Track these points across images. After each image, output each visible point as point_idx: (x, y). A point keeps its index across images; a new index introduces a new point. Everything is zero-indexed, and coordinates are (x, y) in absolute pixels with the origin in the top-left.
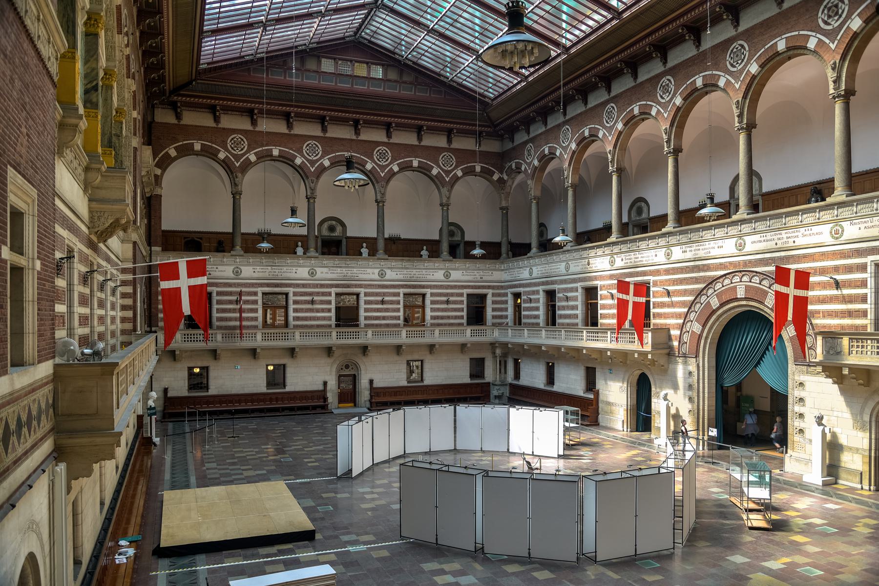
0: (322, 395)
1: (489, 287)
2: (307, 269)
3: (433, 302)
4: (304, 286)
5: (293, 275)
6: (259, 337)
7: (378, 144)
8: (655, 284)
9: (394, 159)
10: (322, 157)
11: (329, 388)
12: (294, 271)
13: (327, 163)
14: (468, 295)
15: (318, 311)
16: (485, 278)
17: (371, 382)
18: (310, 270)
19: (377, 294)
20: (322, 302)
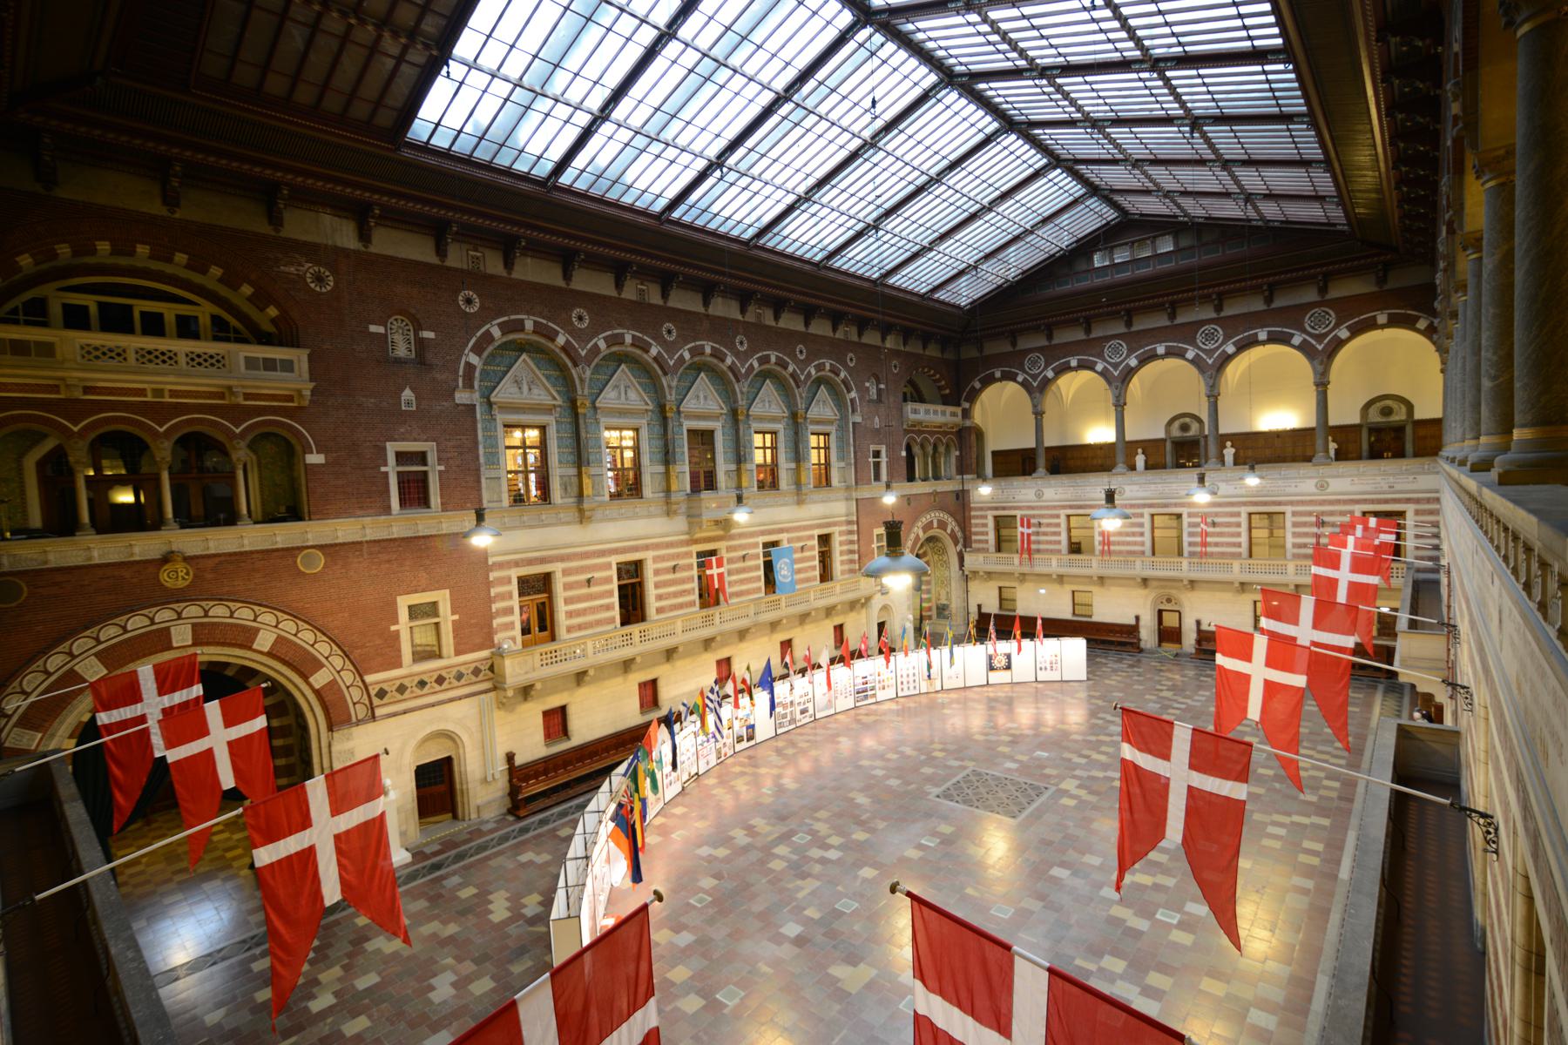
0: (1132, 630)
1: (1408, 501)
3: (1295, 525)
6: (1054, 562)
9: (1227, 338)
10: (1128, 356)
11: (1142, 623)
13: (1133, 362)
16: (1398, 487)
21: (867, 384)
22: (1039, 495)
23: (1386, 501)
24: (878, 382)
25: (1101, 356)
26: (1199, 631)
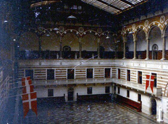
0: (63, 98)
1: (111, 66)
4: (59, 67)
5: (56, 64)
7: (80, 26)
8: (158, 74)
14: (105, 69)
15: (62, 74)
17: (77, 94)
19: (79, 69)
22: (40, 64)
23: (108, 67)
26: (77, 95)
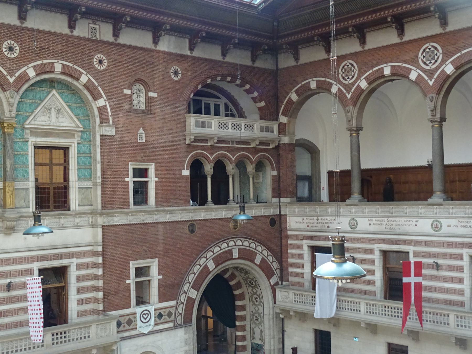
2: (430, 221)
4: (426, 244)
5: (411, 229)
10: (443, 61)
12: (414, 223)
15: (445, 280)
18: (433, 222)
20: (451, 268)
21: (127, 92)
24: (148, 89)
25: (414, 61)
